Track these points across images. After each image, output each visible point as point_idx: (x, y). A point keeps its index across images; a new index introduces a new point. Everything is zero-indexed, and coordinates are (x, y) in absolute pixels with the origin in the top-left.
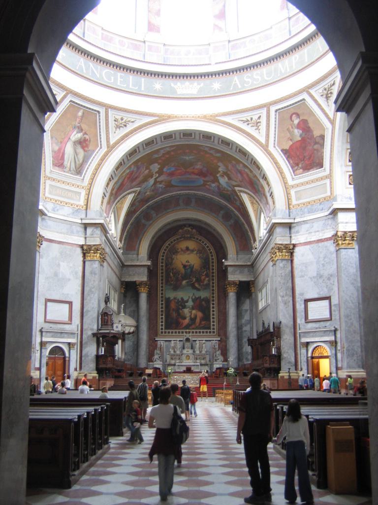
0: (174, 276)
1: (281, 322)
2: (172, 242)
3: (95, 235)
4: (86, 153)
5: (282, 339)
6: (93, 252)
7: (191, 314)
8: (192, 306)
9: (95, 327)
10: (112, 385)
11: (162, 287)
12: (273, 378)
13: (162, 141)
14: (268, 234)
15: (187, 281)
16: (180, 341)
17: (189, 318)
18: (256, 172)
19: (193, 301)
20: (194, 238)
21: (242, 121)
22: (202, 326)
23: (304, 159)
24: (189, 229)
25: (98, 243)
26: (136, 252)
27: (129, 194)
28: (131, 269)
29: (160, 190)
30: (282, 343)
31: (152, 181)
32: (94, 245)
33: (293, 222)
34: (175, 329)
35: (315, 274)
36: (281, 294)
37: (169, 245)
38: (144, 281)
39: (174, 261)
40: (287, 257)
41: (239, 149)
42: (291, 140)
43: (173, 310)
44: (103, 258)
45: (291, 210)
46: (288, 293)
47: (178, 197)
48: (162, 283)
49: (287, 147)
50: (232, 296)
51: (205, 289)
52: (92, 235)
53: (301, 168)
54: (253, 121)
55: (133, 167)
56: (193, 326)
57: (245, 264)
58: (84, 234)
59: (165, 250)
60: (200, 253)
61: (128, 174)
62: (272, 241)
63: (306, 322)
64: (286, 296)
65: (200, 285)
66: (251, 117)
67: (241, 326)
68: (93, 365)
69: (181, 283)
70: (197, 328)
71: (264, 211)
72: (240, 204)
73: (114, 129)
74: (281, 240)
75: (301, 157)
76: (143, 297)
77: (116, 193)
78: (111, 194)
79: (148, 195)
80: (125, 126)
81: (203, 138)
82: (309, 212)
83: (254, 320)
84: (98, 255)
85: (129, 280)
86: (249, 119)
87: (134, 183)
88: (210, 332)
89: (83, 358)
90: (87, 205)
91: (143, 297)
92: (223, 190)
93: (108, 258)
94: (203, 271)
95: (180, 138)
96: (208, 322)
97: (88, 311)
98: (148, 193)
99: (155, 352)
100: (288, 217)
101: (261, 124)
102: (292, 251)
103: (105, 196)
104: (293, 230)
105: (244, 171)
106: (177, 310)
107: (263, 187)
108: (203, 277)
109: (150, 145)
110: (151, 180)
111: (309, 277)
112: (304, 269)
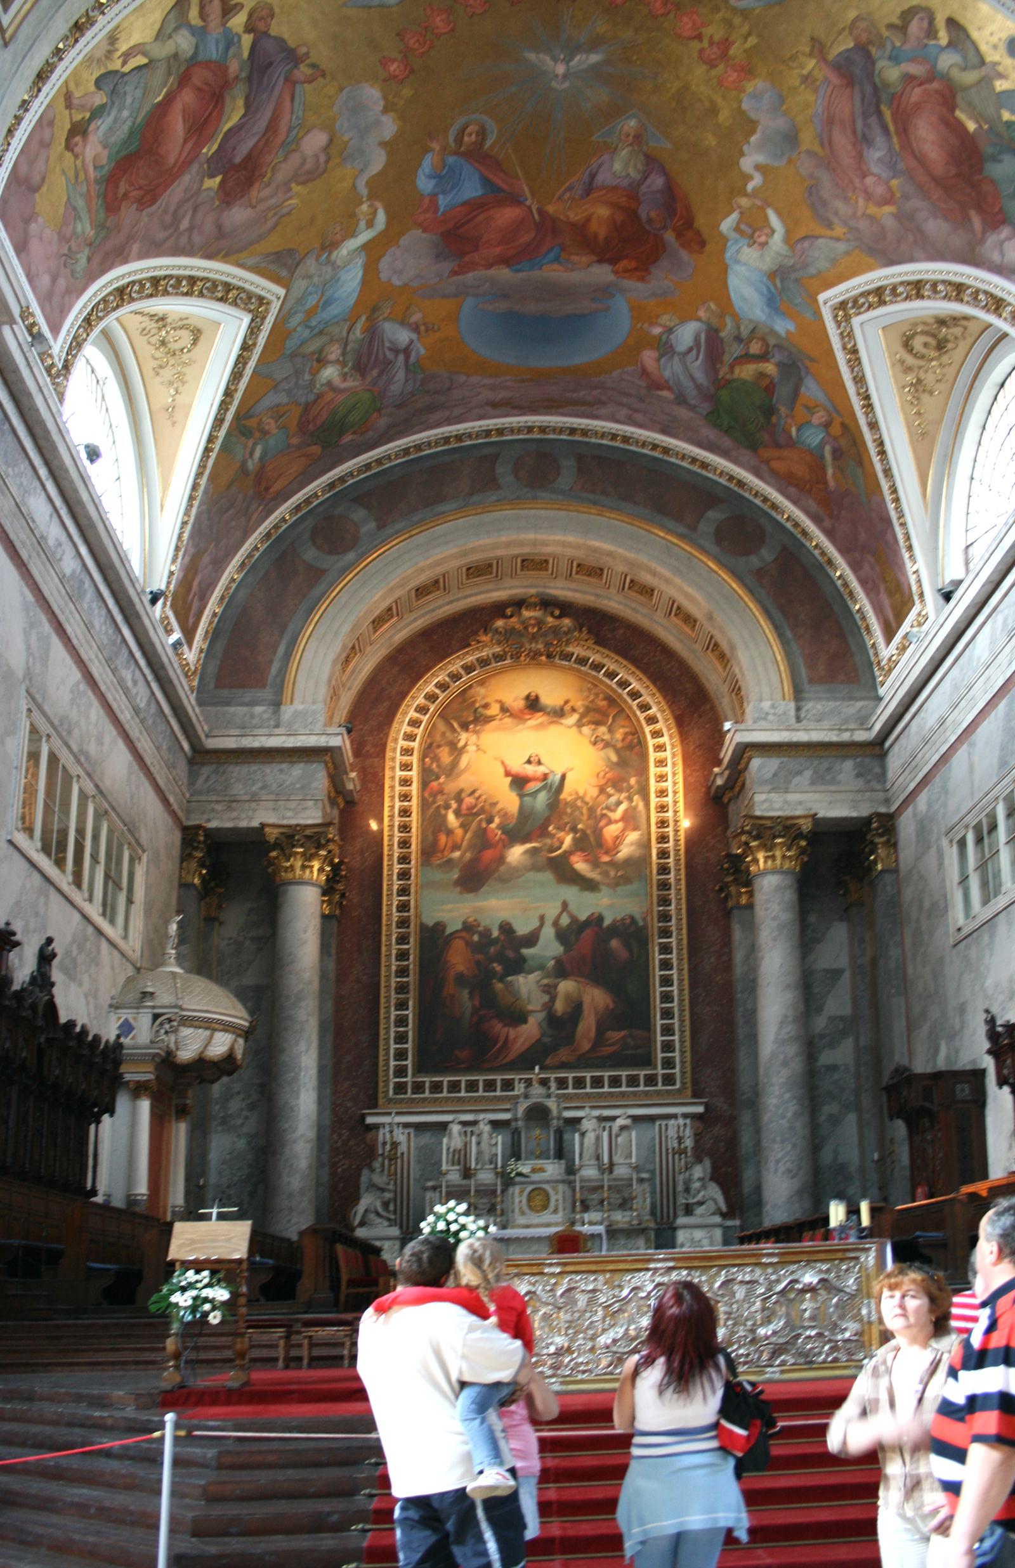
8: (559, 962)
19: (562, 936)
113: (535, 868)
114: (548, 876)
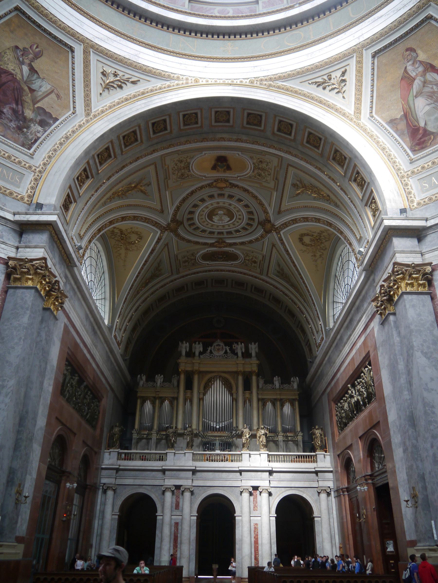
32: (32, 260)
40: (421, 289)
101: (347, 83)
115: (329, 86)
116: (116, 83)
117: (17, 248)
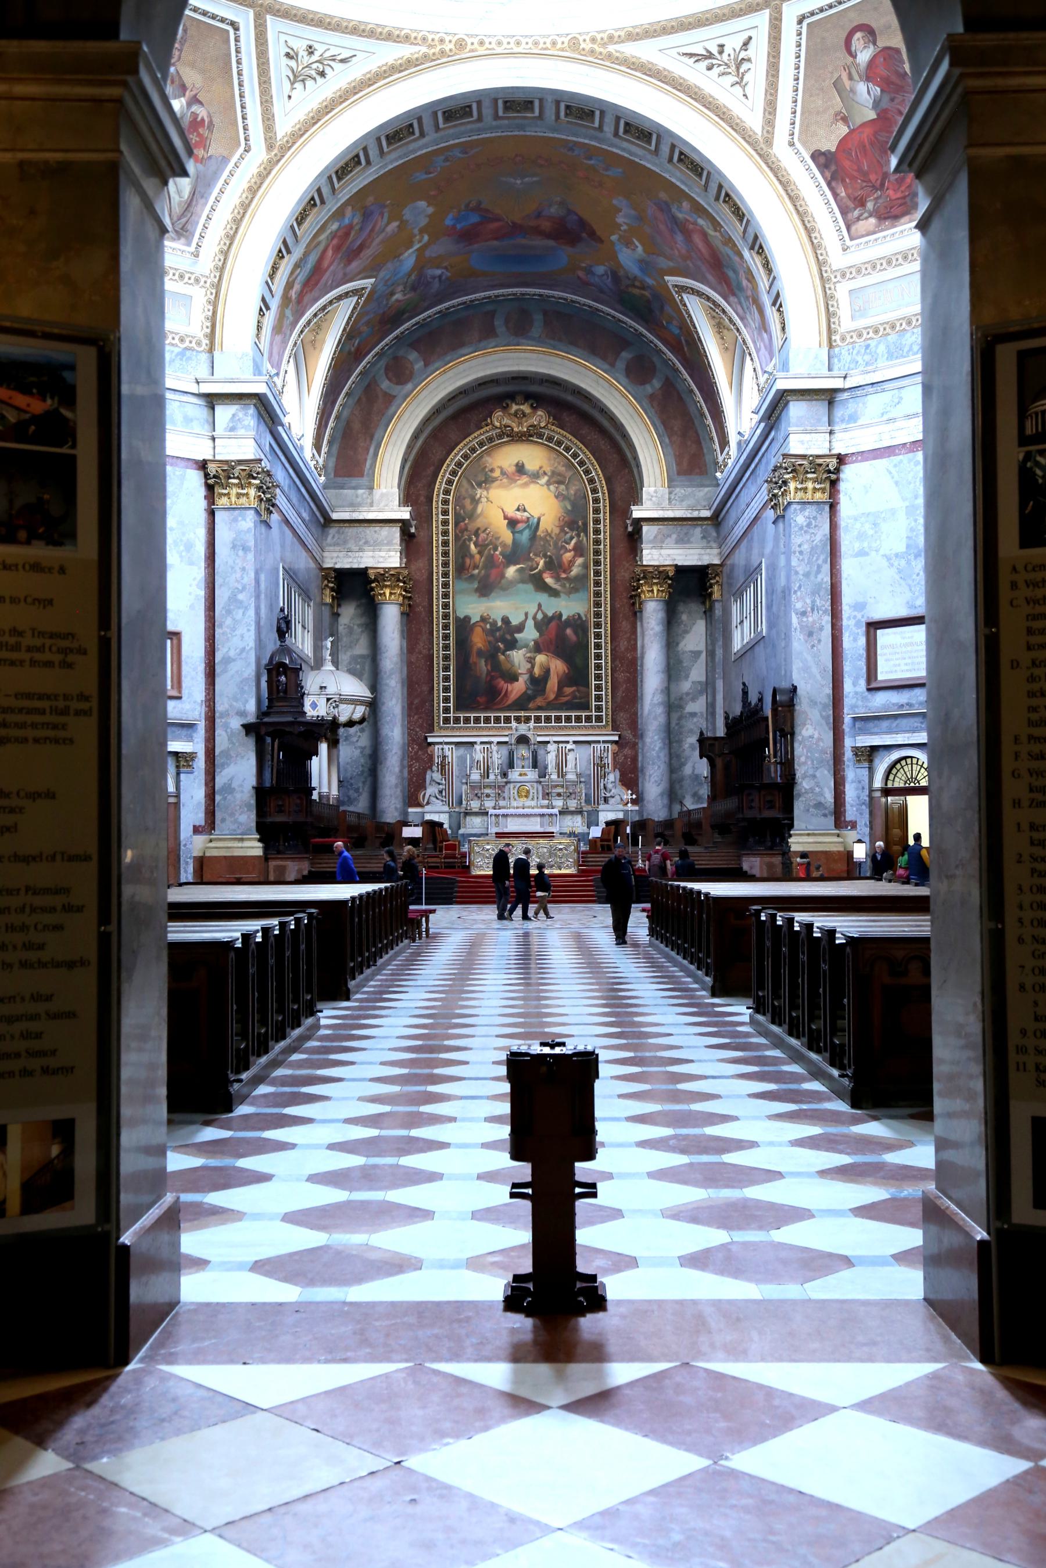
0: (480, 553)
1: (794, 689)
2: (473, 450)
3: (241, 432)
4: (198, 165)
5: (798, 738)
6: (236, 481)
7: (533, 667)
8: (536, 642)
9: (251, 707)
10: (306, 873)
11: (446, 585)
12: (771, 848)
13: (437, 129)
14: (762, 425)
15: (518, 566)
16: (499, 743)
17: (526, 677)
18: (734, 229)
19: (538, 626)
20: (540, 436)
21: (691, 55)
22: (565, 699)
23: (882, 185)
24: (526, 408)
25: (252, 457)
26: (364, 481)
27: (339, 298)
28: (351, 531)
29: (436, 285)
30: (799, 750)
31: (409, 259)
32: (240, 462)
33: (841, 386)
34: (486, 709)
35: (902, 548)
36: (799, 605)
37: (466, 457)
38: (390, 568)
39: (479, 510)
40: (818, 496)
41: (681, 153)
42: (845, 120)
43: (480, 653)
44: (268, 500)
45: (837, 350)
46: (818, 602)
47: (490, 308)
48: (445, 575)
49: (830, 144)
50: (653, 612)
51: (575, 590)
52: (232, 429)
53: (871, 216)
54: (725, 57)
55: (349, 212)
56: (539, 701)
57: (695, 514)
58: (207, 427)
59: (454, 473)
60: (559, 483)
61: (334, 235)
62: (774, 449)
63: (869, 690)
64: (813, 610)
65: (557, 578)
66: (721, 41)
67: (681, 699)
68: (248, 818)
69: (502, 576)
70: (550, 706)
71: (754, 355)
72: (680, 328)
73: (287, 85)
74: (802, 442)
75: (873, 177)
76: (391, 616)
77: (301, 296)
78: (286, 298)
79: (397, 301)
80: (322, 74)
81: (566, 115)
82: (891, 356)
83: (720, 684)
84: (252, 492)
85: (348, 566)
86: (715, 50)
87: (355, 265)
88: (588, 719)
89: (218, 798)
90: (212, 336)
91: (391, 616)
92: (627, 286)
93: (281, 500)
94: (568, 536)
95: (496, 117)
96: (582, 689)
97: (227, 660)
98: (398, 296)
99: (428, 777)
100: (825, 372)
102: (833, 477)
103: (268, 308)
104: (839, 413)
105: (695, 223)
106: (492, 655)
107: (751, 277)
108: (568, 556)
109: (400, 139)
110: (406, 254)
111: (884, 556)
112: (871, 532)
113: (523, 581)
114: (530, 587)
115: (720, 65)
116: (314, 66)
117: (213, 439)
